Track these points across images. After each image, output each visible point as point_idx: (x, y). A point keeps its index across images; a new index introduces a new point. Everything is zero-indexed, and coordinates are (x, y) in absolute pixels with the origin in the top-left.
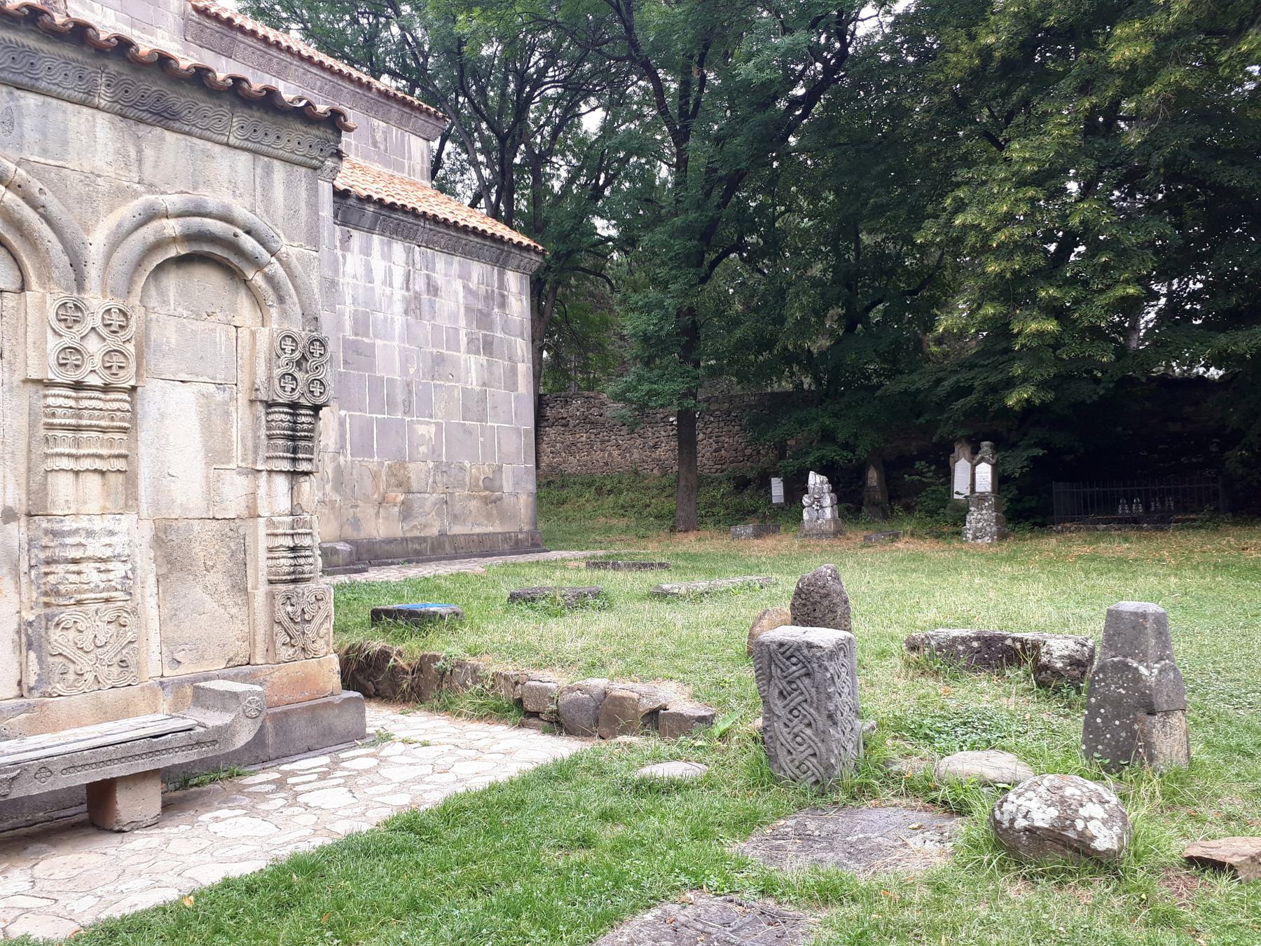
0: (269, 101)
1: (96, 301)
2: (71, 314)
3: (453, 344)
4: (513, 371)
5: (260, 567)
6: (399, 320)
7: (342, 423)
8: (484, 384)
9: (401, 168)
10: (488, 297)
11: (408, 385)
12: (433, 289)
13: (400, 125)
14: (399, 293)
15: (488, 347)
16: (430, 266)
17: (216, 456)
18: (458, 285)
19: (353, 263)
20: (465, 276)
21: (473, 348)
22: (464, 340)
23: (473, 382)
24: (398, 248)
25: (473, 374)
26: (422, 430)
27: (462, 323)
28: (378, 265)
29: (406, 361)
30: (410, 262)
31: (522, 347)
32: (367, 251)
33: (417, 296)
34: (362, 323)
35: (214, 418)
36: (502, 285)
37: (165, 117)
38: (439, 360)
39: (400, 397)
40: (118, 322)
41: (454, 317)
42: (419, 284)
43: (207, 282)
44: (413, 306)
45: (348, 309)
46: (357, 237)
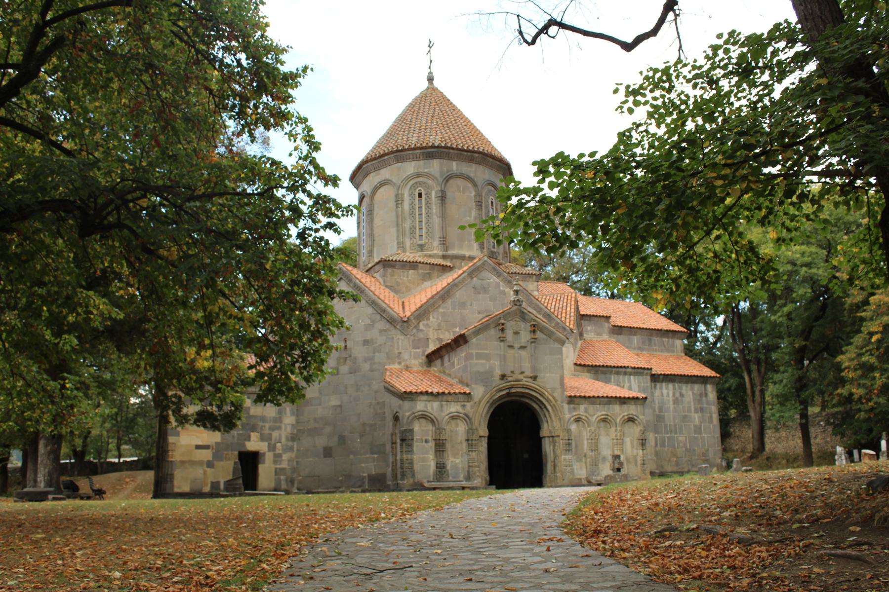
0: (637, 398)
1: (619, 428)
2: (616, 430)
3: (689, 411)
4: (711, 417)
5: (639, 462)
6: (672, 407)
7: (656, 438)
8: (701, 422)
9: (673, 351)
10: (701, 395)
11: (675, 426)
12: (682, 395)
13: (673, 338)
14: (671, 398)
15: (702, 410)
16: (680, 388)
17: (633, 447)
18: (690, 393)
19: (657, 393)
20: (692, 389)
21: (696, 411)
22: (693, 409)
23: (697, 422)
24: (671, 386)
25: (697, 420)
26: (680, 439)
27: (692, 404)
28: (665, 391)
29: (674, 418)
30: (674, 388)
31: (714, 409)
32: (661, 388)
33: (677, 399)
34: (661, 409)
35: (632, 442)
36: (705, 389)
37: (625, 403)
38: (685, 417)
39: (673, 428)
40: (621, 431)
41: (689, 403)
42: (678, 395)
43: (630, 423)
44: (676, 402)
45: (657, 406)
46: (658, 385)
